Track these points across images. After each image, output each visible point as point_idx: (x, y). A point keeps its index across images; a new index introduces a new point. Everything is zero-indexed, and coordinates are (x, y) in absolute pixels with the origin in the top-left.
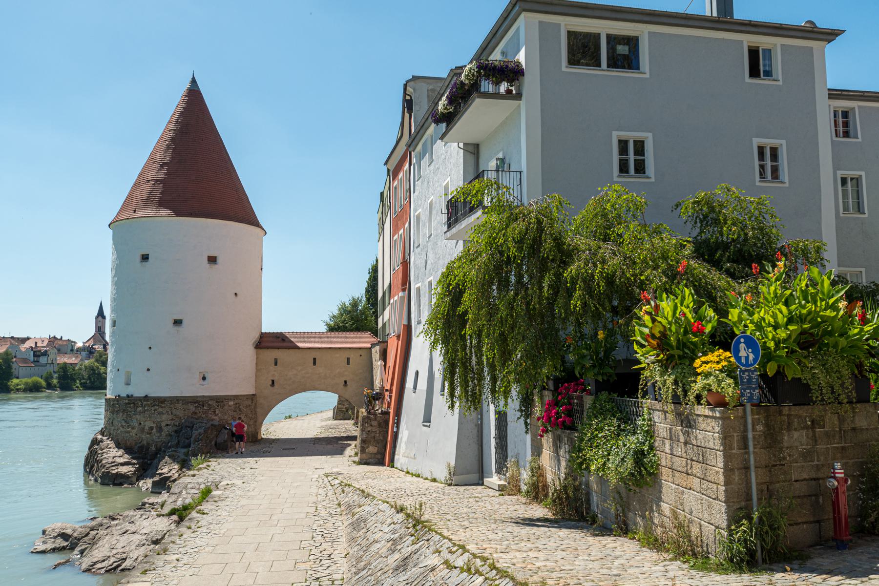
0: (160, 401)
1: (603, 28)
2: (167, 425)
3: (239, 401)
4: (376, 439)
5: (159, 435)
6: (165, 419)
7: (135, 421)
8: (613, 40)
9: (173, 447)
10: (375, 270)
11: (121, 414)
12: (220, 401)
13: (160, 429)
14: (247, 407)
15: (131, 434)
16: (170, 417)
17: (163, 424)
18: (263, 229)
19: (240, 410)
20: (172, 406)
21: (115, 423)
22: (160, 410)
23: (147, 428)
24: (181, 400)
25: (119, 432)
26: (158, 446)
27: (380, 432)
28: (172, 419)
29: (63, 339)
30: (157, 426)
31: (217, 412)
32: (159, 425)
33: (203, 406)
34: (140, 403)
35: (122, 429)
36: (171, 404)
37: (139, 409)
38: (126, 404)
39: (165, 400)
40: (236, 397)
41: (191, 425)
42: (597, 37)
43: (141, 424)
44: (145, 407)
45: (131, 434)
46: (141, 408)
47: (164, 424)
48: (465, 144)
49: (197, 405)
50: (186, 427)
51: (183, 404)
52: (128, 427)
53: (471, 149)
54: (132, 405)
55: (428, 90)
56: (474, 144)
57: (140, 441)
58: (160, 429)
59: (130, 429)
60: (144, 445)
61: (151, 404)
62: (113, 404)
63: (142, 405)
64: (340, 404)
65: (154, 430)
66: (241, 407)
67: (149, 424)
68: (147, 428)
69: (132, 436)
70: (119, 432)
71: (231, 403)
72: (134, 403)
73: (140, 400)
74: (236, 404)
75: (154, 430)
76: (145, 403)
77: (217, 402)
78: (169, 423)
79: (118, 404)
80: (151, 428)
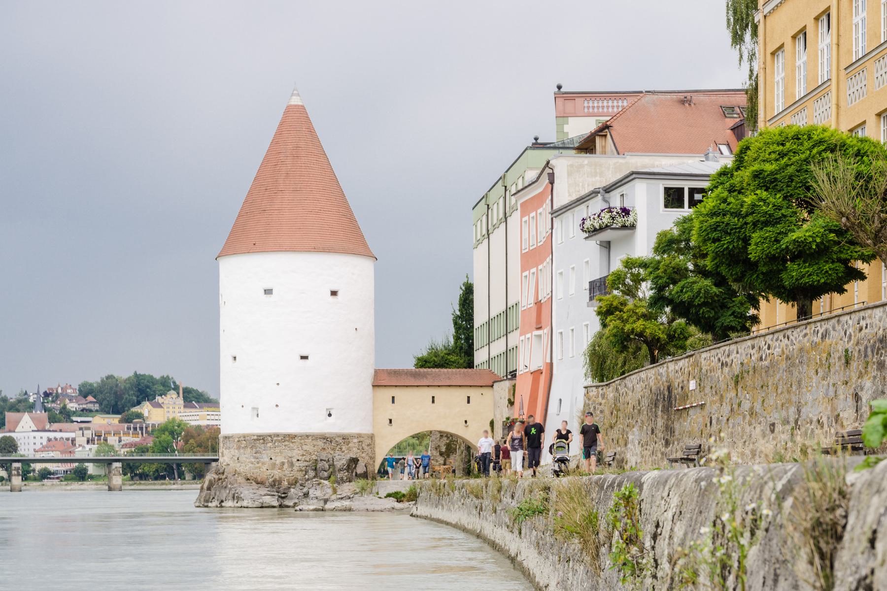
0: (290, 438)
1: (686, 185)
2: (298, 460)
3: (362, 439)
5: (290, 469)
6: (296, 454)
7: (265, 456)
8: (692, 191)
10: (469, 290)
11: (249, 450)
12: (346, 438)
13: (292, 465)
14: (368, 445)
16: (301, 452)
17: (294, 460)
19: (363, 449)
20: (302, 441)
21: (242, 458)
22: (291, 445)
23: (278, 462)
24: (310, 435)
25: (247, 468)
26: (290, 480)
28: (303, 455)
30: (288, 461)
31: (343, 449)
32: (290, 459)
33: (331, 442)
34: (270, 439)
36: (301, 440)
37: (270, 444)
38: (255, 440)
39: (296, 436)
40: (359, 436)
41: (327, 459)
42: (683, 189)
43: (271, 459)
44: (275, 443)
45: (261, 470)
46: (270, 444)
47: (296, 460)
48: (601, 242)
49: (325, 441)
50: (321, 460)
51: (312, 440)
52: (258, 463)
53: (605, 245)
54: (261, 441)
55: (568, 166)
56: (607, 242)
57: (272, 475)
58: (292, 465)
59: (260, 464)
60: (276, 479)
62: (238, 441)
63: (272, 441)
65: (286, 466)
66: (363, 445)
67: (279, 460)
68: (278, 462)
69: (263, 472)
70: (247, 468)
71: (356, 440)
72: (263, 439)
73: (270, 436)
74: (360, 442)
75: (286, 466)
76: (275, 438)
77: (343, 439)
78: (300, 458)
79: (245, 440)
80: (283, 463)
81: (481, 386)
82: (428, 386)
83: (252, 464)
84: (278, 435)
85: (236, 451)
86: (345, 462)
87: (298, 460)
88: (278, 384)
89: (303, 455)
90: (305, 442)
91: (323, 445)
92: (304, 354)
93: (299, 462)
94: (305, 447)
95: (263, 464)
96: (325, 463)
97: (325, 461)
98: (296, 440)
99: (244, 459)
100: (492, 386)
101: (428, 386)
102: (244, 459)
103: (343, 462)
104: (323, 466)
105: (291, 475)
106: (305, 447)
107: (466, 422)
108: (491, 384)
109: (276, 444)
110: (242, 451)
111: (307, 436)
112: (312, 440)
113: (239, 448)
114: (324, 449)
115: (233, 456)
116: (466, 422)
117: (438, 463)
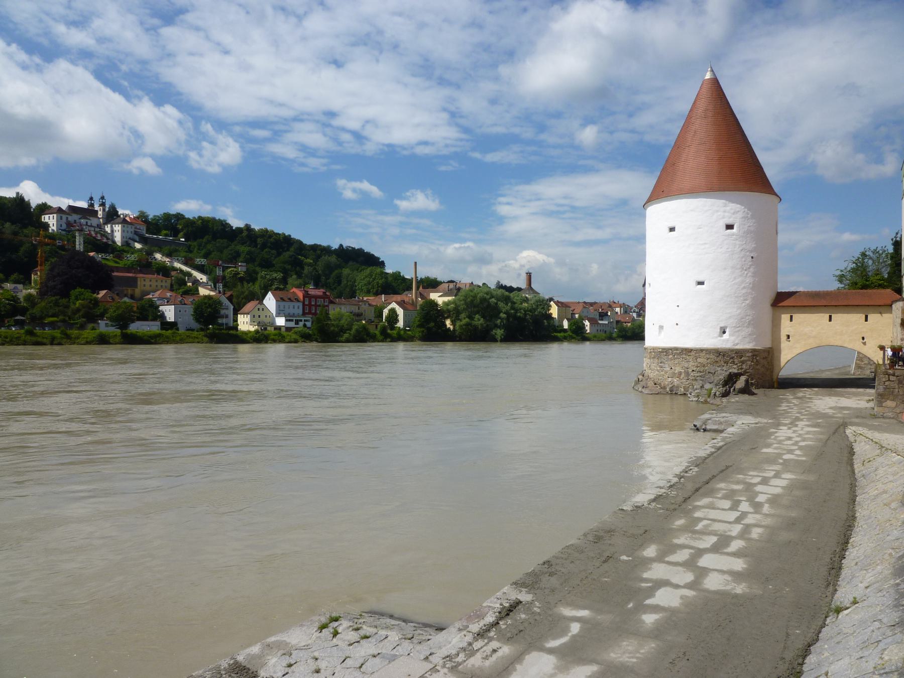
0: (688, 351)
2: (693, 371)
4: (894, 394)
5: (686, 378)
6: (691, 365)
9: (698, 389)
14: (764, 358)
15: (664, 377)
18: (778, 196)
20: (698, 354)
21: (653, 367)
27: (899, 388)
29: (620, 303)
30: (685, 371)
33: (724, 355)
34: (671, 351)
35: (657, 373)
41: (713, 372)
43: (671, 368)
44: (674, 356)
45: (664, 377)
46: (671, 356)
47: (691, 371)
50: (709, 373)
51: (706, 354)
52: (662, 371)
58: (687, 374)
61: (680, 353)
62: (650, 352)
64: (859, 360)
67: (678, 369)
76: (675, 351)
77: (736, 353)
78: (695, 369)
80: (680, 373)
81: (880, 306)
82: (825, 306)
83: (658, 371)
84: (676, 349)
85: (649, 360)
86: (723, 378)
87: (693, 371)
88: (678, 306)
89: (697, 367)
90: (699, 355)
91: (716, 358)
92: (700, 280)
93: (694, 372)
94: (699, 360)
95: (666, 372)
96: (712, 375)
97: (712, 373)
98: (693, 353)
99: (653, 367)
100: (891, 306)
101: (825, 306)
102: (653, 367)
103: (720, 377)
104: (709, 378)
105: (687, 383)
106: (699, 360)
107: (863, 338)
108: (890, 303)
109: (676, 356)
110: (652, 360)
111: (702, 350)
112: (706, 354)
113: (650, 358)
114: (717, 361)
115: (648, 364)
116: (863, 338)
117: (863, 363)
